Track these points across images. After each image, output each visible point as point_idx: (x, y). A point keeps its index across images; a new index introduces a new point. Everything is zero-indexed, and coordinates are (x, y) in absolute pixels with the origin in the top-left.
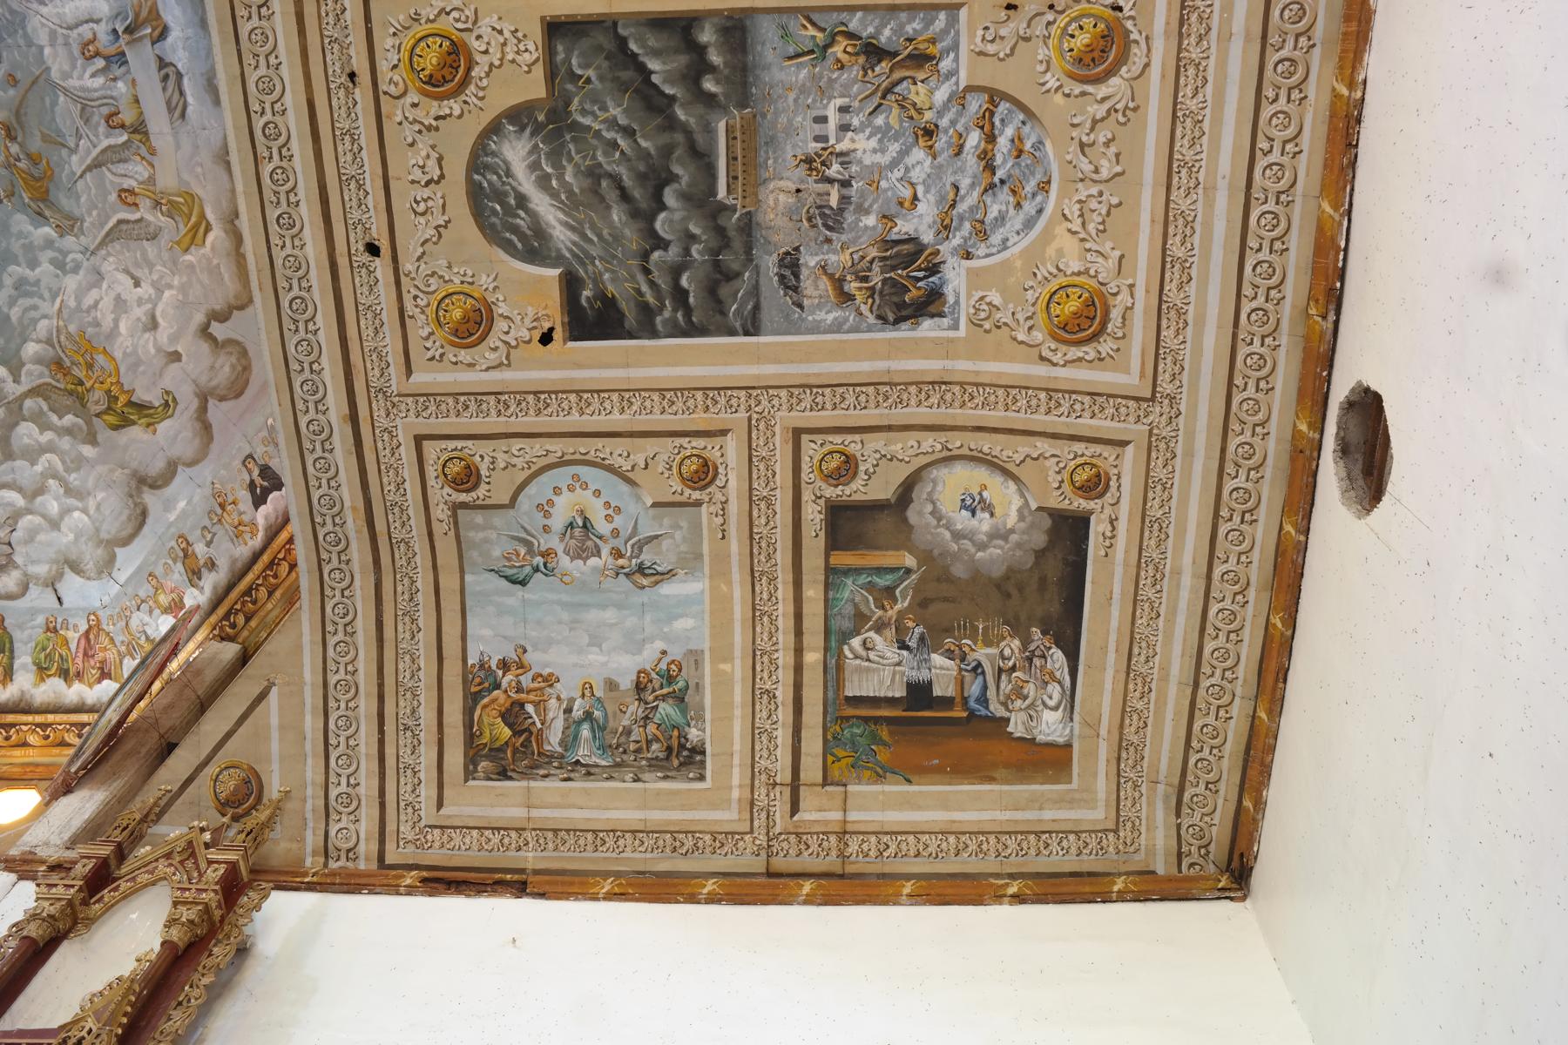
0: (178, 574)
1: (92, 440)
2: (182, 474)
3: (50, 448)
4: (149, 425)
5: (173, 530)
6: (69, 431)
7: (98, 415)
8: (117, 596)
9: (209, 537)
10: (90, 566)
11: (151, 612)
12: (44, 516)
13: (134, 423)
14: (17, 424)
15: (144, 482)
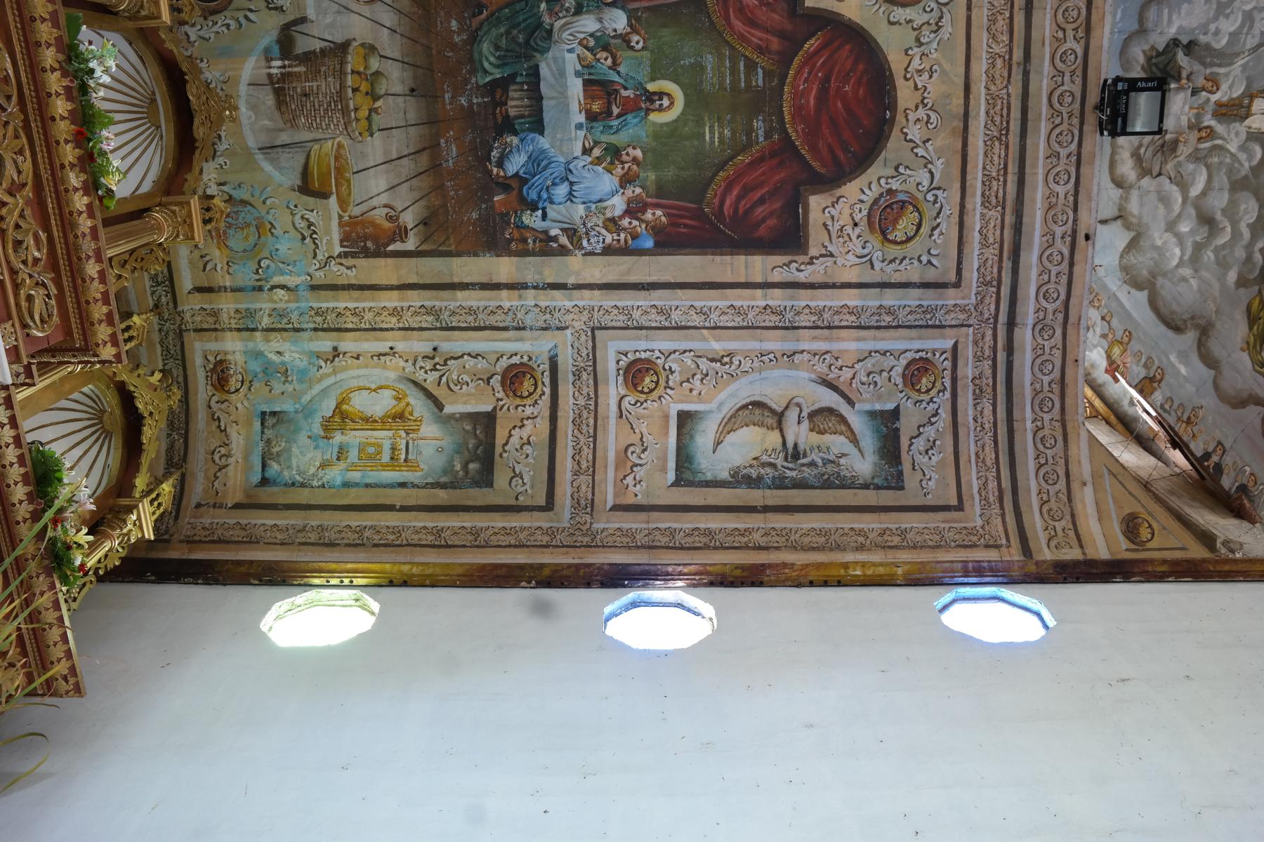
0: (1139, 372)
1: (1242, 282)
2: (1208, 374)
3: (1236, 234)
4: (1248, 343)
5: (1164, 359)
6: (1249, 259)
7: (1260, 292)
8: (1105, 287)
9: (1167, 407)
10: (1132, 259)
11: (1104, 336)
12: (1179, 216)
13: (1251, 329)
14: (1258, 200)
15: (1205, 331)
